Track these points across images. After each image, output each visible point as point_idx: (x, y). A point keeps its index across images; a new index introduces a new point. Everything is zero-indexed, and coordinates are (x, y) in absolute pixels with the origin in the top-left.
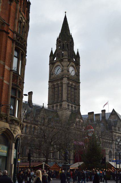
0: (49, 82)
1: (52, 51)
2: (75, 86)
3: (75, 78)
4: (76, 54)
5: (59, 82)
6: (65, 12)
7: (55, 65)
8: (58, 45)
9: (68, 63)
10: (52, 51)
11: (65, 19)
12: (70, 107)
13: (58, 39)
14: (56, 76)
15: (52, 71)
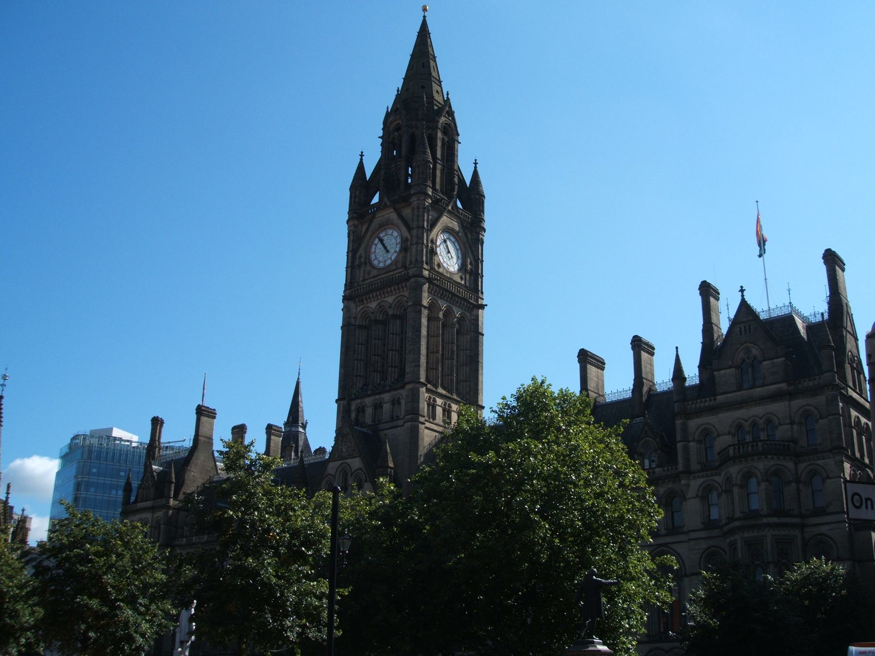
0: (345, 299)
1: (361, 168)
2: (461, 319)
3: (463, 282)
4: (468, 181)
5: (390, 299)
6: (425, 9)
7: (374, 225)
8: (390, 139)
9: (432, 214)
10: (361, 168)
11: (424, 34)
12: (439, 411)
13: (388, 115)
14: (374, 272)
15: (361, 251)
